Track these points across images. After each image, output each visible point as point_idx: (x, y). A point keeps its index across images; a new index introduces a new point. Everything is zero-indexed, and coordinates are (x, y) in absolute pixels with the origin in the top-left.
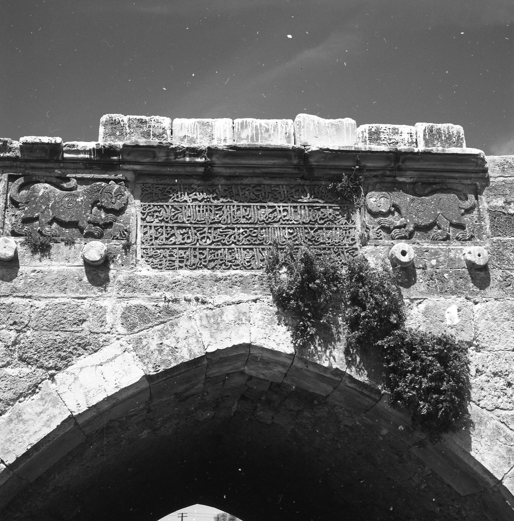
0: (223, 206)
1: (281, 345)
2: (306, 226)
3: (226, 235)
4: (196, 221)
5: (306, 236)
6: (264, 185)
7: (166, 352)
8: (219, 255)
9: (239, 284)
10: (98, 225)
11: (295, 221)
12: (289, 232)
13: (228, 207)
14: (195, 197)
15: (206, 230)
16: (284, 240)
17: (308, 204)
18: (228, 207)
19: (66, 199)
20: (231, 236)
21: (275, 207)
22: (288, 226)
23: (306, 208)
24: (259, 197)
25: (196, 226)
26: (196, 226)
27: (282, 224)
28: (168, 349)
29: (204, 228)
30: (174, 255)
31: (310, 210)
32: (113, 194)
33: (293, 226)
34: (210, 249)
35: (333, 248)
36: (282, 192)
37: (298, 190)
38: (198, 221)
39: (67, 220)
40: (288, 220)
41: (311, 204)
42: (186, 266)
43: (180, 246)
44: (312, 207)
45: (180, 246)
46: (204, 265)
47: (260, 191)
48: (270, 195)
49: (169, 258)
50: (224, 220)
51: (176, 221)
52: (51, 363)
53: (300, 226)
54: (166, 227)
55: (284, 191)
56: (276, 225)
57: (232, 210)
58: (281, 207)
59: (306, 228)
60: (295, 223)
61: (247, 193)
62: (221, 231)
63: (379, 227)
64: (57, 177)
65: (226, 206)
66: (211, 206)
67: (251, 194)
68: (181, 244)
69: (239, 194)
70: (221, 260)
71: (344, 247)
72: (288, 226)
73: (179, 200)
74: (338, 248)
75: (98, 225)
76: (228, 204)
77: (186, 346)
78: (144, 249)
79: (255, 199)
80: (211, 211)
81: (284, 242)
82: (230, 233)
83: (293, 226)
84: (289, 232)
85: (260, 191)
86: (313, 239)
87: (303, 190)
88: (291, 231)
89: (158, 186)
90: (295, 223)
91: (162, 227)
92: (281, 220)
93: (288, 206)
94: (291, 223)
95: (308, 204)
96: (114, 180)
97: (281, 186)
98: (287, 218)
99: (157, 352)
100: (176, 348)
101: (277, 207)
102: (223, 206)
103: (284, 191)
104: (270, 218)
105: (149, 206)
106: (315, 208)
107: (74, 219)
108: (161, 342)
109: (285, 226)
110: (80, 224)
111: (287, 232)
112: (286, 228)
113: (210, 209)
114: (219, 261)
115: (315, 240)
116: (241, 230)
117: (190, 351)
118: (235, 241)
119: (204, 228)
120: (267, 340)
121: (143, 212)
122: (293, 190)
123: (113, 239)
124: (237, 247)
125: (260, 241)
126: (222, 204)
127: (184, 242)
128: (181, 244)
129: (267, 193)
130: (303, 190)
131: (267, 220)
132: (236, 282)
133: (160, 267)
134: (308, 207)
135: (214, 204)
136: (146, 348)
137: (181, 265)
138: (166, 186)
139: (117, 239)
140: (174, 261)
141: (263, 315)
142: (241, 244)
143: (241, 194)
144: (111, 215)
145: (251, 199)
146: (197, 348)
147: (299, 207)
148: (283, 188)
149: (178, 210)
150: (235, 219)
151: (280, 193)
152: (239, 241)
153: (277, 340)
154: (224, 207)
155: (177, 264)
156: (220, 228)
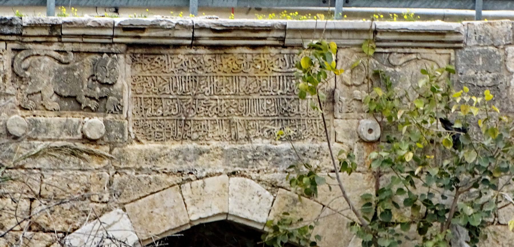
0: (207, 77)
1: (254, 214)
2: (283, 97)
3: (209, 107)
4: (182, 93)
5: (283, 107)
6: (246, 54)
7: (156, 219)
8: (203, 126)
9: (219, 157)
10: (94, 98)
11: (274, 92)
12: (267, 104)
13: (212, 78)
14: (182, 68)
15: (190, 101)
16: (262, 111)
17: (287, 74)
18: (212, 78)
19: (65, 73)
20: (214, 107)
21: (255, 77)
22: (267, 97)
23: (285, 78)
24: (240, 67)
25: (182, 97)
26: (182, 97)
27: (261, 95)
28: (157, 216)
29: (189, 99)
30: (162, 127)
31: (287, 80)
32: (107, 68)
33: (271, 97)
34: (194, 120)
35: (307, 120)
36: (263, 62)
37: (278, 59)
38: (184, 92)
39: (67, 94)
40: (266, 91)
41: (290, 74)
42: (172, 137)
43: (168, 118)
44: (291, 76)
45: (168, 118)
46: (188, 137)
47: (242, 60)
48: (252, 65)
49: (158, 129)
50: (208, 92)
51: (164, 92)
52: (60, 228)
53: (277, 97)
54: (155, 98)
55: (264, 61)
56: (256, 96)
57: (215, 80)
58: (261, 78)
59: (282, 99)
60: (274, 94)
61: (230, 63)
62: (205, 102)
63: (351, 100)
64: (56, 51)
65: (210, 77)
66: (195, 77)
67: (234, 64)
68: (168, 115)
69: (222, 65)
70: (204, 131)
71: (317, 118)
72: (267, 97)
73: (167, 70)
74: (312, 120)
75: (94, 98)
76: (211, 74)
77: (173, 214)
78: (135, 120)
79: (237, 69)
80: (195, 81)
81: (262, 113)
82: (213, 105)
83: (271, 97)
84: (267, 104)
85: (242, 60)
86: (290, 110)
87: (283, 60)
88: (269, 103)
89: (146, 56)
90: (274, 94)
91: (150, 98)
92: (260, 91)
93: (267, 77)
94: (268, 93)
95: (287, 74)
96: (109, 54)
97: (262, 55)
98: (266, 89)
99: (148, 219)
100: (165, 216)
101: (258, 78)
102: (207, 77)
103: (264, 61)
104: (250, 89)
105: (139, 77)
106: (292, 78)
107: (73, 94)
108: (151, 211)
109: (263, 97)
110: (78, 99)
111: (265, 104)
112: (265, 100)
113: (195, 80)
114: (202, 132)
115: (291, 112)
116: (223, 102)
117: (177, 218)
118: (217, 112)
119: (189, 99)
120: (243, 209)
121: (133, 83)
122: (274, 59)
123: (108, 113)
124: (219, 118)
125: (240, 112)
126: (206, 75)
127: (171, 113)
128: (168, 115)
129: (248, 63)
130: (283, 60)
131: (248, 91)
132: (218, 155)
133: (149, 138)
134: (287, 76)
135: (199, 75)
136: (138, 216)
137: (168, 136)
138: (154, 56)
139: (112, 113)
140: (161, 132)
141: (240, 187)
142: (222, 115)
143: (223, 64)
144: (105, 89)
145: (233, 69)
146: (182, 216)
147: (278, 78)
148: (264, 57)
149: (165, 81)
150: (218, 90)
151: (261, 62)
152: (220, 112)
153: (252, 210)
154: (209, 78)
155: (165, 135)
156: (203, 99)
